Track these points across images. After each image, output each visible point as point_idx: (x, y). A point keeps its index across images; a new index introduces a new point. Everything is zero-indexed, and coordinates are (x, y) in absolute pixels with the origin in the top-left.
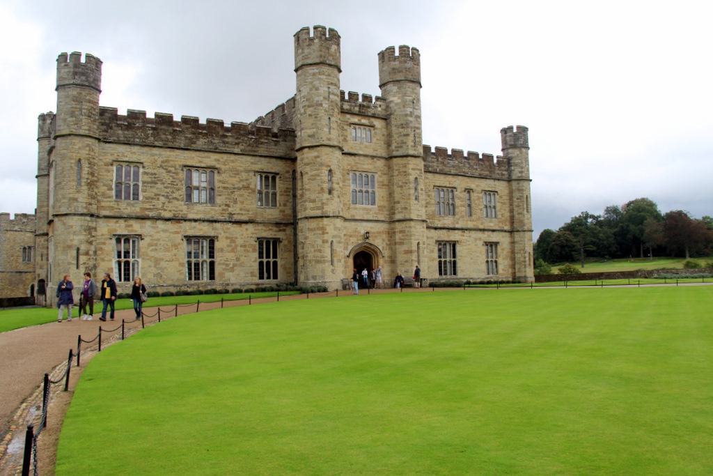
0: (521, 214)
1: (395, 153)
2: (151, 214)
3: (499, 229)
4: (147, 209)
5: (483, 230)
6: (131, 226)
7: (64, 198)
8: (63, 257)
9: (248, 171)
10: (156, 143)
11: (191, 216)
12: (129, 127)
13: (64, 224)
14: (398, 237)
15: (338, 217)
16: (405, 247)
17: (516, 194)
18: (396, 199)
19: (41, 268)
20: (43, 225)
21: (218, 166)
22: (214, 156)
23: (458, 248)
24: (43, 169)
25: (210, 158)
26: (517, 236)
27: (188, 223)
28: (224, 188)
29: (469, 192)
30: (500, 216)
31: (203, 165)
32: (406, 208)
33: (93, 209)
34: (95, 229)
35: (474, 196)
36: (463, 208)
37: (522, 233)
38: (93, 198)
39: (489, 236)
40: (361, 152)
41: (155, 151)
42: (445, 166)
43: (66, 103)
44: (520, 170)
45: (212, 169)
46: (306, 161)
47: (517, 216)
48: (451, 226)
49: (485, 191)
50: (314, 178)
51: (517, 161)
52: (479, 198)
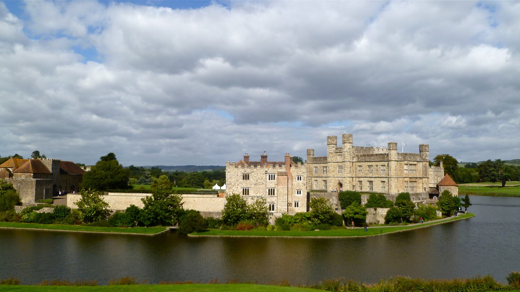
2: (319, 176)
3: (386, 177)
5: (381, 178)
11: (324, 176)
12: (316, 160)
15: (329, 177)
23: (373, 183)
27: (323, 178)
29: (377, 166)
30: (386, 173)
33: (311, 176)
34: (311, 179)
35: (378, 167)
36: (375, 171)
38: (310, 174)
39: (382, 179)
40: (340, 161)
42: (370, 159)
45: (326, 167)
48: (371, 177)
49: (382, 165)
52: (380, 168)
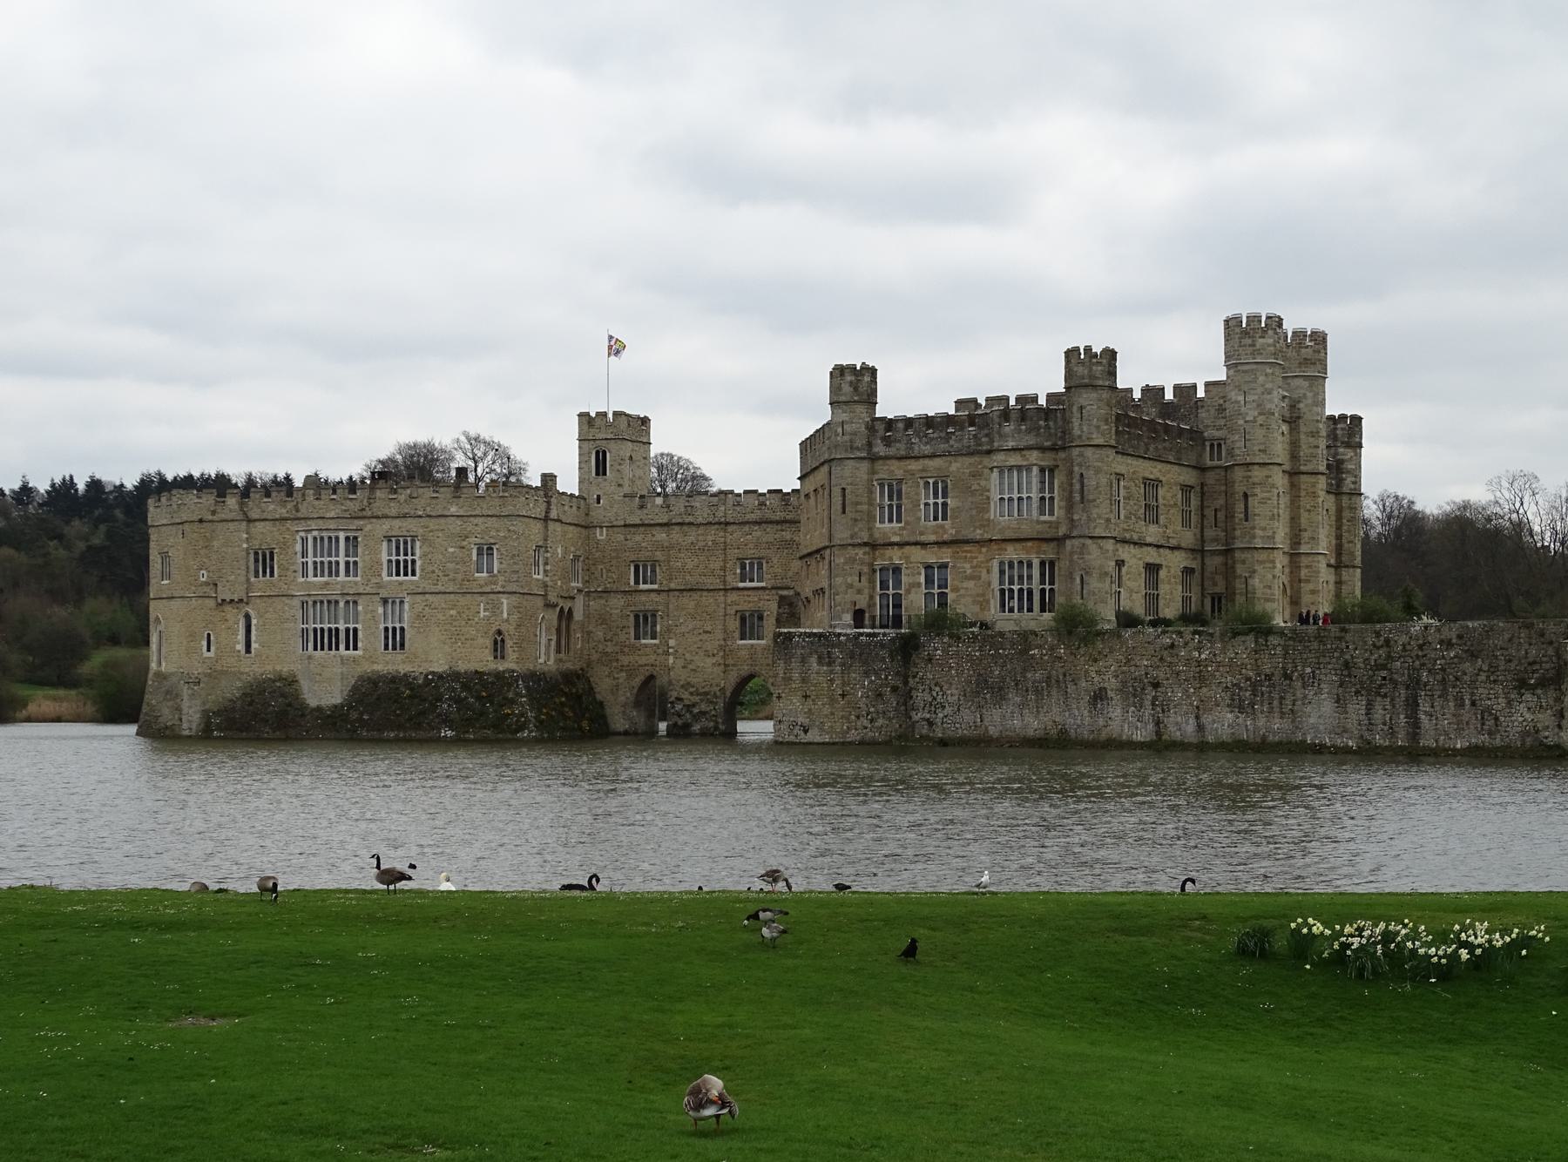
0: (1351, 542)
1: (1303, 468)
4: (1125, 530)
6: (1117, 550)
7: (1100, 518)
8: (1100, 585)
9: (1176, 484)
10: (1130, 451)
11: (1149, 540)
13: (1101, 548)
14: (1304, 573)
16: (1311, 586)
17: (1346, 514)
18: (1303, 527)
19: (859, 592)
20: (861, 530)
21: (1161, 478)
22: (1160, 466)
24: (858, 449)
25: (1155, 467)
26: (1345, 573)
28: (1165, 505)
31: (1152, 477)
32: (1314, 538)
37: (1351, 570)
41: (1129, 460)
43: (1099, 408)
44: (1353, 479)
46: (1256, 480)
47: (1346, 545)
50: (1263, 502)
51: (1349, 467)
